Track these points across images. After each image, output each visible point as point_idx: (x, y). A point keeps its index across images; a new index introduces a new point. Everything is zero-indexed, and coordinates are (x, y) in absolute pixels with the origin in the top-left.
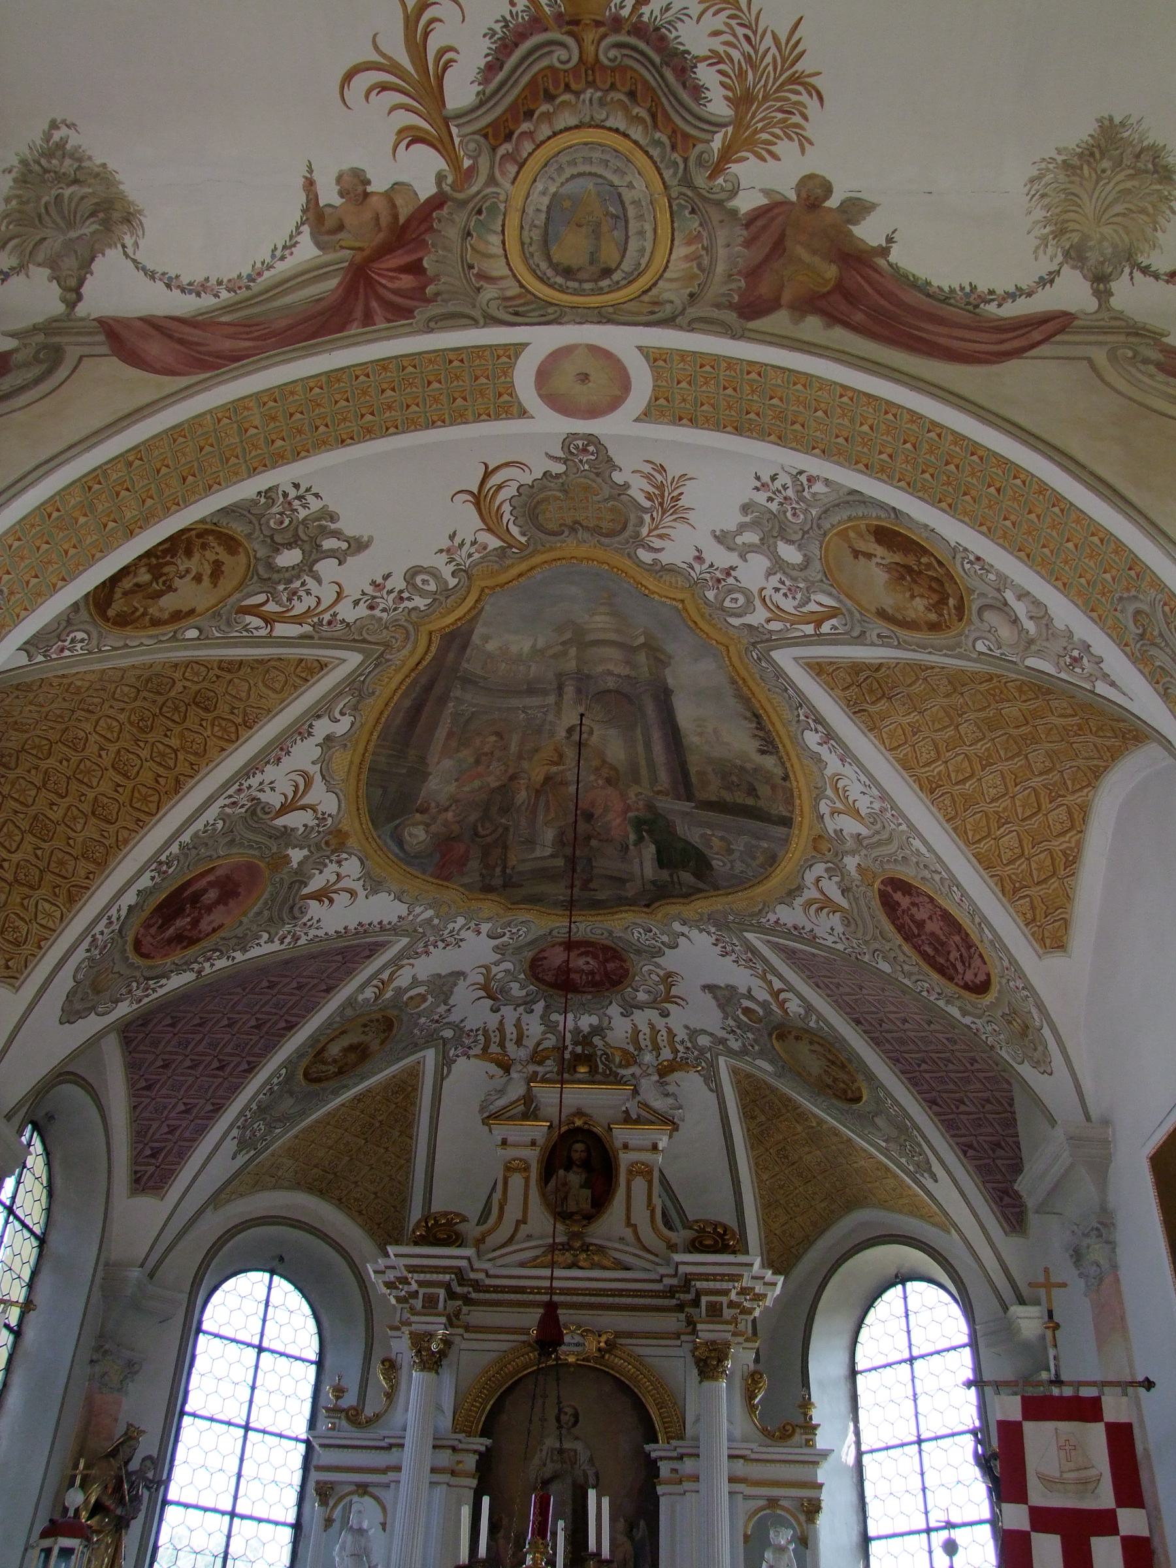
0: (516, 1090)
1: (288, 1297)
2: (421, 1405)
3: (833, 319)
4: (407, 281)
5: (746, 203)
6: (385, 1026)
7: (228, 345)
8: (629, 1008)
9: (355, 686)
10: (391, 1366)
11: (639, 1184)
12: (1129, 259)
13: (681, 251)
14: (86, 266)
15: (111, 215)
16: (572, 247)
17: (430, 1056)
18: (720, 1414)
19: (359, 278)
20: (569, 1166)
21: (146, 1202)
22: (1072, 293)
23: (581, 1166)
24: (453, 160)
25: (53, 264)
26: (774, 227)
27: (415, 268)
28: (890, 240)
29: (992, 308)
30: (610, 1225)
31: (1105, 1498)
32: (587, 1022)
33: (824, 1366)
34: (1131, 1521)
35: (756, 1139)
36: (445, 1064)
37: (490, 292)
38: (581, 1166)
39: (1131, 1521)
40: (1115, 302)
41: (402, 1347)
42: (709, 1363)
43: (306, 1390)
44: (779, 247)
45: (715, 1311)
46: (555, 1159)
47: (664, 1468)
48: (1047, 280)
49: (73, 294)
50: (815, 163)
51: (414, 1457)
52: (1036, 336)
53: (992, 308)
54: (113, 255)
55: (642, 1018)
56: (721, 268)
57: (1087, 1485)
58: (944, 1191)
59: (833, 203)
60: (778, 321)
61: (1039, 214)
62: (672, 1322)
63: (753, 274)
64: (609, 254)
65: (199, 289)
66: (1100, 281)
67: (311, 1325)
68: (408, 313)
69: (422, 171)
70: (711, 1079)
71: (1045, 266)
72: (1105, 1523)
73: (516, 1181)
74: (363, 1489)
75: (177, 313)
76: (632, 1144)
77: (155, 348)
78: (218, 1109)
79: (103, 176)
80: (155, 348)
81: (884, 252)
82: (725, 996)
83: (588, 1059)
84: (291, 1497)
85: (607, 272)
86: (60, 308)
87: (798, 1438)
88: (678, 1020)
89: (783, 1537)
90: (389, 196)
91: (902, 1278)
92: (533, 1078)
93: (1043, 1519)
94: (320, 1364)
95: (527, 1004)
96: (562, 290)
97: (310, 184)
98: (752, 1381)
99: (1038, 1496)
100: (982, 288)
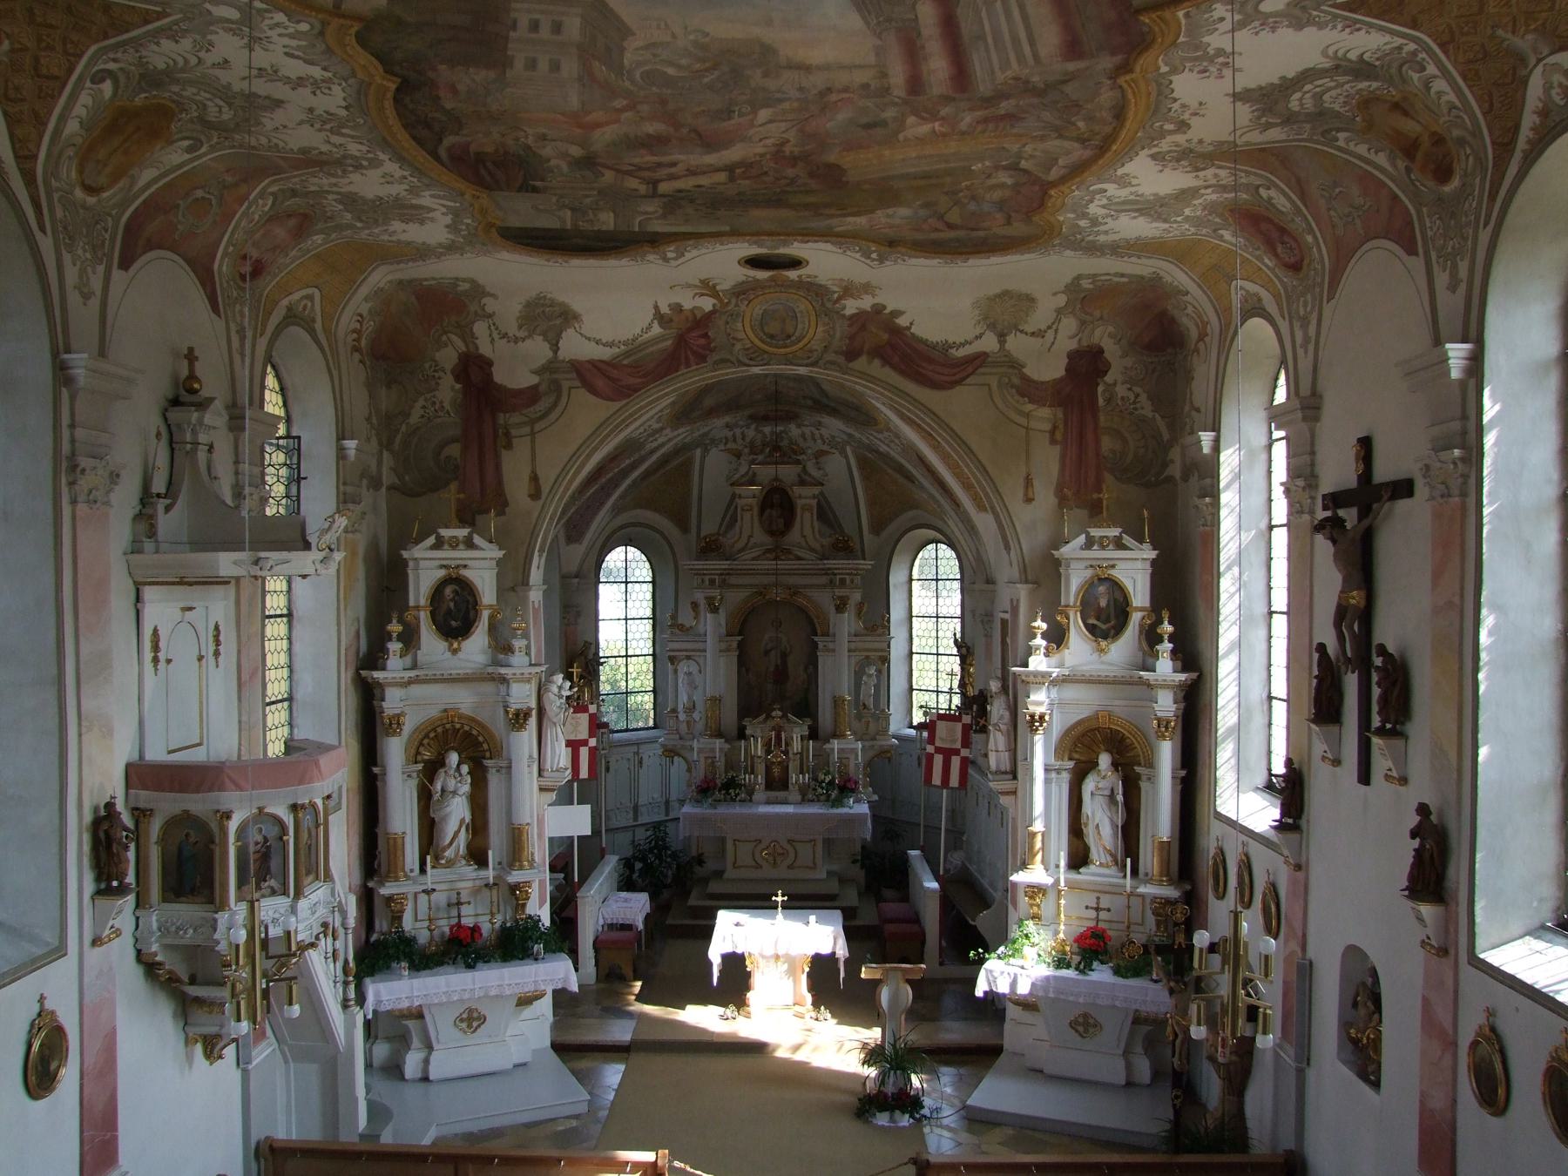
0: (743, 470)
1: (633, 552)
2: (711, 626)
3: (886, 361)
4: (702, 341)
5: (848, 312)
6: (677, 451)
7: (632, 381)
8: (799, 426)
9: (673, 403)
10: (695, 605)
11: (807, 515)
13: (820, 329)
14: (559, 336)
15: (568, 317)
16: (773, 327)
17: (698, 452)
18: (846, 624)
19: (681, 340)
20: (772, 506)
21: (573, 547)
22: (989, 343)
23: (778, 506)
24: (721, 301)
25: (544, 334)
26: (861, 321)
27: (706, 336)
29: (953, 351)
30: (794, 535)
31: (958, 745)
32: (779, 428)
33: (896, 577)
34: (965, 752)
35: (866, 478)
36: (706, 451)
37: (738, 346)
38: (778, 507)
39: (965, 752)
41: (700, 596)
42: (840, 608)
43: (649, 596)
44: (863, 327)
45: (843, 582)
46: (766, 503)
47: (821, 646)
48: (979, 337)
49: (555, 348)
50: (876, 301)
51: (711, 642)
52: (970, 369)
53: (953, 351)
54: (571, 331)
55: (807, 431)
56: (838, 335)
57: (954, 741)
58: (950, 523)
60: (861, 363)
62: (824, 580)
63: (852, 338)
64: (791, 330)
65: (610, 345)
66: (1002, 337)
67: (647, 565)
68: (702, 358)
69: (707, 304)
70: (843, 453)
71: (978, 331)
72: (957, 752)
73: (747, 515)
74: (688, 658)
75: (605, 358)
76: (804, 497)
77: (600, 383)
78: (602, 504)
79: (563, 304)
80: (600, 383)
81: (909, 328)
82: (850, 436)
83: (777, 448)
84: (650, 643)
85: (789, 337)
86: (551, 354)
87: (880, 631)
88: (823, 431)
89: (872, 671)
90: (692, 311)
92: (753, 462)
93: (938, 750)
94: (653, 582)
95: (748, 427)
96: (770, 345)
97: (656, 307)
98: (860, 606)
99: (938, 743)
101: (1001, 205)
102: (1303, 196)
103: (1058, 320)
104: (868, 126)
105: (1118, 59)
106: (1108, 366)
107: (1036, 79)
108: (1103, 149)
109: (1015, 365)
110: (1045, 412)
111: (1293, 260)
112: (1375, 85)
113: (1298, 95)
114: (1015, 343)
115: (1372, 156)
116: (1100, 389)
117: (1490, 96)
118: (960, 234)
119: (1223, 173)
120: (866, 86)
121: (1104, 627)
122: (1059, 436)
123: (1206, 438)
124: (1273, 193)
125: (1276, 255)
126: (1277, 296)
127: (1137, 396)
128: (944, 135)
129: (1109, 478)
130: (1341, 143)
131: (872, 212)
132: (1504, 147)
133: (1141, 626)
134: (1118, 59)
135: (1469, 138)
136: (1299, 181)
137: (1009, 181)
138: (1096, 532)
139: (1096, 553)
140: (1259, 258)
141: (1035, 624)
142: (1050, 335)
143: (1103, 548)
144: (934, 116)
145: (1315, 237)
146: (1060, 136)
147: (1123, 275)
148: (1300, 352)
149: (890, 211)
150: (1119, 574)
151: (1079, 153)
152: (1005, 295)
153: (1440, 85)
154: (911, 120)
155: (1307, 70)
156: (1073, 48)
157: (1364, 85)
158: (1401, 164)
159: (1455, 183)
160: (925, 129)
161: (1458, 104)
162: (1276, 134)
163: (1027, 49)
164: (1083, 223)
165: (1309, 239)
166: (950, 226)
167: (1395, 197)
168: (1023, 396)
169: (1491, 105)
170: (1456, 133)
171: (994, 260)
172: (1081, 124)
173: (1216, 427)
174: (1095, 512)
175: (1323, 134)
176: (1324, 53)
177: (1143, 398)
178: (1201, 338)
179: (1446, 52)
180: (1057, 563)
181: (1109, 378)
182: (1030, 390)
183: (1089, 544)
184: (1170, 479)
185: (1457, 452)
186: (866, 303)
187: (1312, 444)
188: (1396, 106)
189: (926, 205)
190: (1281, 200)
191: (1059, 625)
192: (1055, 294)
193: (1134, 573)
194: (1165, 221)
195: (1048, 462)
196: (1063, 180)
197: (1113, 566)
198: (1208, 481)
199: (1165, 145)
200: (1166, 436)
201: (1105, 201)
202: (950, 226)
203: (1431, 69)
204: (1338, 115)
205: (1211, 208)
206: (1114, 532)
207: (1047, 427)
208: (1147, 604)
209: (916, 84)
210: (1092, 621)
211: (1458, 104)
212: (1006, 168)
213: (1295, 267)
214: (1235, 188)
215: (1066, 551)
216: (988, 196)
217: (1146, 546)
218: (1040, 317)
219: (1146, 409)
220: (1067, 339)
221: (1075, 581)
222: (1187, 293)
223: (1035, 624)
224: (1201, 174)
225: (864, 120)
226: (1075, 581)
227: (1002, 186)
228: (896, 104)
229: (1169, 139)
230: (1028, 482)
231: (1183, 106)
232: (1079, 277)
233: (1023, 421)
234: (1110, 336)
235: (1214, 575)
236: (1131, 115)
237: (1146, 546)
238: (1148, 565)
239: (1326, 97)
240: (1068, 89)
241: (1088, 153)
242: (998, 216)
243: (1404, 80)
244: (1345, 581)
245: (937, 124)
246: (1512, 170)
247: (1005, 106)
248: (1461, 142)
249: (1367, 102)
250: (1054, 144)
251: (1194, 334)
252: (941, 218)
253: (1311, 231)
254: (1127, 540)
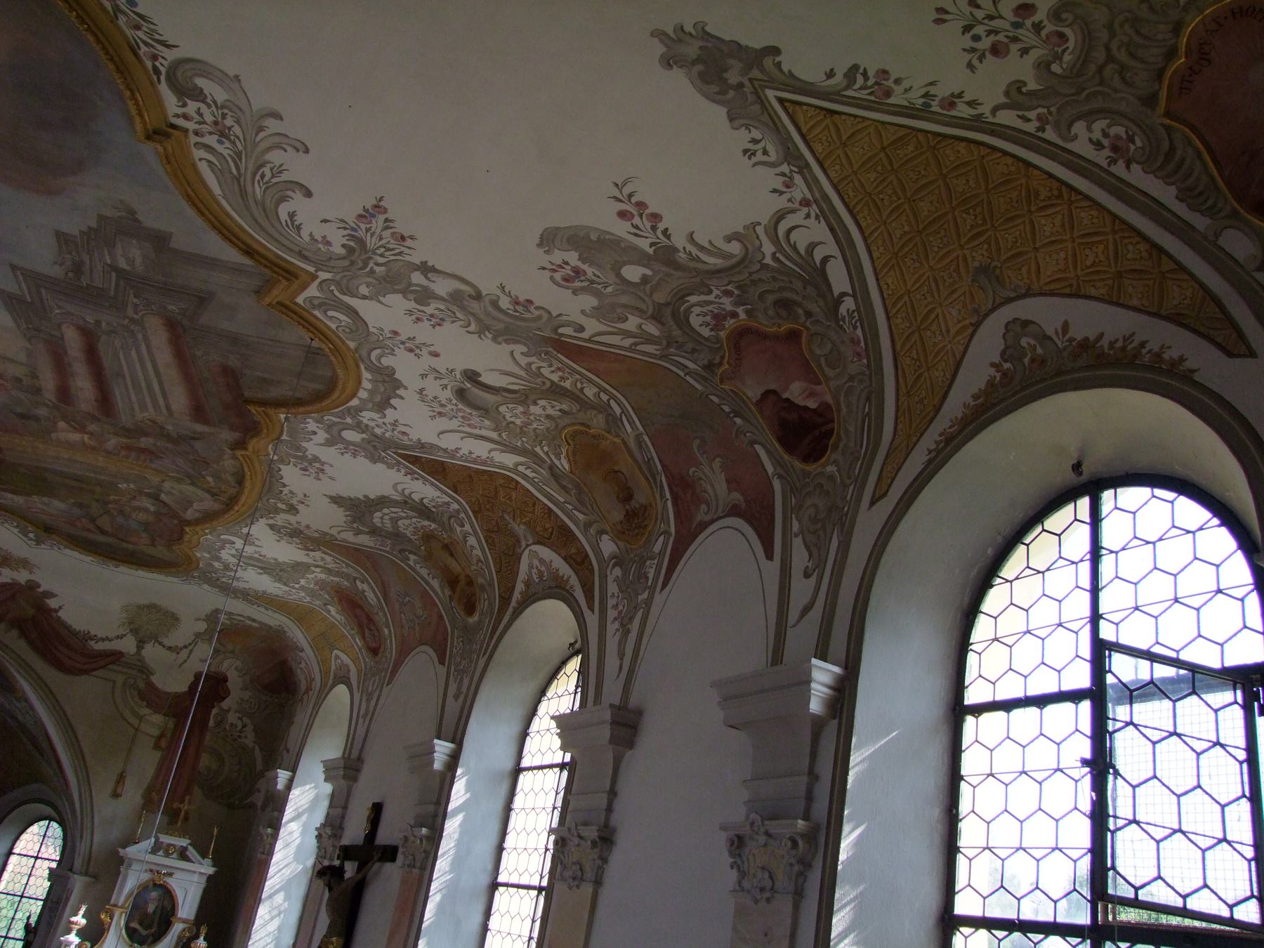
3: (24, 634)
12: (155, 638)
22: (128, 645)
28: (60, 608)
29: (92, 643)
40: (144, 652)
48: (119, 637)
50: (32, 577)
53: (92, 643)
59: (41, 590)
61: (124, 615)
66: (141, 643)
71: (121, 632)
81: (56, 611)
91: (51, 819)
100: (93, 633)
101: (146, 526)
102: (386, 596)
103: (194, 643)
104: (22, 416)
105: (237, 435)
106: (227, 693)
107: (170, 428)
108: (229, 504)
109: (145, 670)
110: (158, 719)
111: (374, 645)
113: (378, 514)
114: (152, 653)
115: (430, 581)
116: (214, 711)
118: (110, 540)
119: (329, 559)
120: (18, 380)
121: (144, 933)
122: (163, 743)
123: (283, 776)
124: (365, 586)
125: (364, 638)
126: (359, 671)
127: (244, 726)
128: (94, 449)
129: (197, 791)
130: (411, 563)
131: (29, 495)
133: (179, 937)
134: (237, 435)
136: (383, 583)
137: (152, 508)
138: (166, 839)
139: (159, 859)
140: (352, 636)
141: (74, 919)
142: (185, 653)
143: (167, 855)
144: (82, 429)
146: (193, 484)
147: (254, 620)
148: (361, 720)
149: (45, 499)
150: (173, 883)
151: (209, 504)
152: (152, 607)
154: (62, 424)
155: (384, 497)
156: (199, 412)
157: (426, 523)
158: (448, 592)
159: (475, 619)
160: (75, 437)
162: (365, 540)
163: (161, 401)
164: (216, 564)
165: (386, 631)
166: (103, 532)
167: (441, 617)
168: (142, 698)
170: (480, 580)
171: (141, 573)
172: (210, 479)
173: (294, 770)
174: (174, 821)
175: (401, 551)
176: (395, 486)
177: (250, 728)
178: (307, 692)
180: (121, 861)
181: (225, 704)
182: (151, 696)
183: (155, 850)
184: (252, 806)
185: (424, 830)
186: (22, 577)
187: (347, 801)
188: (446, 547)
189: (80, 506)
190: (371, 596)
191: (101, 923)
192: (198, 620)
193: (189, 885)
194: (285, 584)
195: (146, 763)
196: (197, 522)
197: (171, 875)
198: (276, 813)
199: (281, 519)
200: (259, 766)
201: (233, 552)
202: (103, 532)
204: (410, 541)
205: (322, 585)
206: (184, 842)
207: (156, 732)
208: (192, 917)
209: (64, 394)
210: (134, 925)
212: (149, 495)
213: (374, 651)
214: (338, 574)
215: (132, 851)
216: (134, 515)
217: (208, 861)
218: (180, 636)
219: (249, 739)
220: (202, 659)
221: (132, 881)
222: (302, 650)
223: (74, 919)
224: (312, 554)
225: (19, 410)
226: (132, 881)
227: (146, 510)
228: (48, 406)
229: (282, 516)
230: (121, 778)
231: (291, 492)
232: (217, 611)
233: (135, 722)
234: (236, 668)
235: (257, 901)
236: (248, 484)
237: (208, 861)
238: (204, 879)
239: (400, 523)
240: (198, 445)
241: (217, 507)
242: (144, 535)
244: (330, 926)
245: (86, 437)
247: (145, 442)
249: (428, 537)
250: (189, 489)
251: (303, 686)
252: (93, 520)
253: (388, 627)
254: (192, 852)
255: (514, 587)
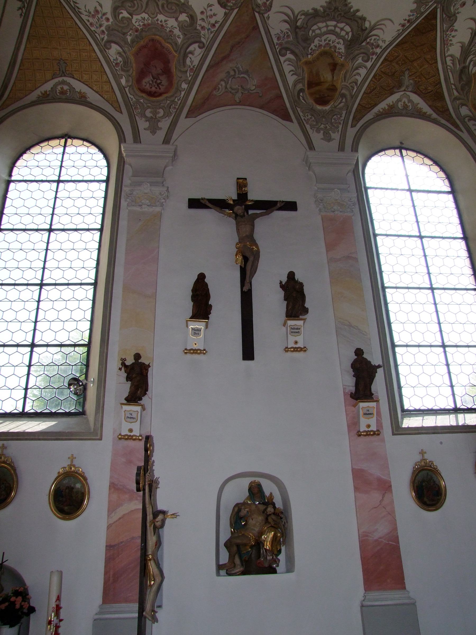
102: (214, 65)
112: (343, 50)
117: (374, 89)
130: (282, 59)
132: (364, 109)
135: (349, 97)
145: (190, 89)
153: (363, 72)
161: (359, 83)
165: (184, 86)
169: (371, 92)
179: (382, 63)
203: (369, 64)
211: (359, 83)
243: (353, 59)
246: (369, 116)
248: (343, 96)
255: (376, 105)
